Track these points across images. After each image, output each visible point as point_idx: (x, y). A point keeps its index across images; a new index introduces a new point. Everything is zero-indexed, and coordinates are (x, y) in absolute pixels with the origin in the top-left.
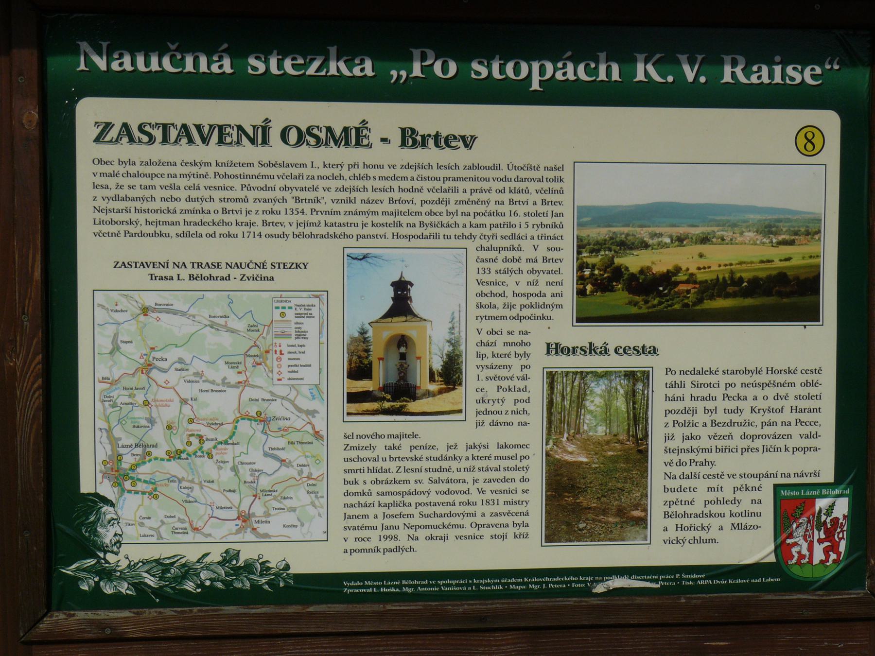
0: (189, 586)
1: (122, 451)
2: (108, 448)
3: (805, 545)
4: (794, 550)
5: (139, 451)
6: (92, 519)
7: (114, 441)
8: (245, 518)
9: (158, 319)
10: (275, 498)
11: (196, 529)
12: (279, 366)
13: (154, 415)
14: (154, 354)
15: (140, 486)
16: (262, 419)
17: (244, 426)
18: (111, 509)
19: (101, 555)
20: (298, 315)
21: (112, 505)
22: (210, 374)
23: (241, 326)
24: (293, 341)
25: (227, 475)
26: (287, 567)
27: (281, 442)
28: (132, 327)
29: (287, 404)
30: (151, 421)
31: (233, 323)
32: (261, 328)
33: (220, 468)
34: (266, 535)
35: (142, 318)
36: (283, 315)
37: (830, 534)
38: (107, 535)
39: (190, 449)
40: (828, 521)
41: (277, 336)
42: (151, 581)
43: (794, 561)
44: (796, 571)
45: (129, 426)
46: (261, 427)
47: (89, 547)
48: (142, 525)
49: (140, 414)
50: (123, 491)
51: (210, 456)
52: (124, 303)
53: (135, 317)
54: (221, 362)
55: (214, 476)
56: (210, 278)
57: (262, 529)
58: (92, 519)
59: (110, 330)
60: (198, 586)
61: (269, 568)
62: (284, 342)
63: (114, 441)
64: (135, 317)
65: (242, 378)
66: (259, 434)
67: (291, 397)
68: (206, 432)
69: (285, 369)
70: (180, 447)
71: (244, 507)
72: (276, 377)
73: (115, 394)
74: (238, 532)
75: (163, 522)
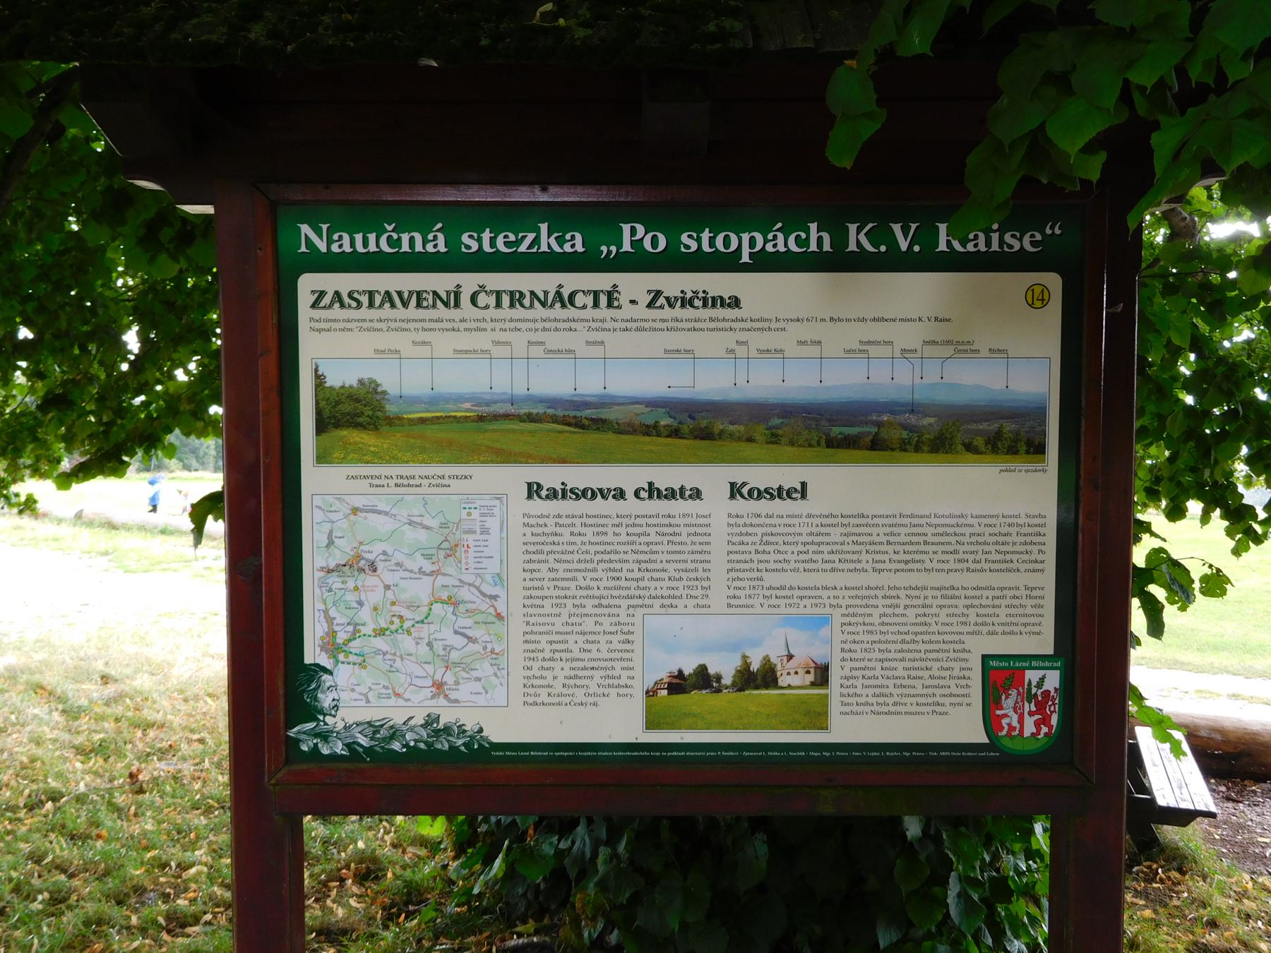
0: (396, 746)
1: (336, 628)
2: (325, 625)
3: (1015, 718)
4: (1004, 722)
5: (350, 628)
6: (313, 686)
7: (330, 620)
8: (439, 686)
9: (365, 518)
10: (464, 670)
11: (398, 695)
12: (467, 558)
13: (363, 598)
14: (362, 547)
15: (352, 658)
16: (453, 602)
17: (437, 608)
18: (330, 677)
19: (321, 718)
20: (482, 515)
21: (331, 673)
22: (409, 564)
23: (434, 523)
24: (478, 536)
25: (423, 649)
26: (481, 730)
27: (468, 622)
28: (344, 524)
29: (473, 589)
30: (360, 603)
31: (428, 521)
32: (450, 525)
33: (417, 643)
34: (456, 701)
35: (352, 517)
36: (469, 514)
37: (1041, 707)
38: (326, 700)
39: (393, 627)
40: (1039, 693)
41: (465, 532)
42: (364, 741)
43: (1004, 732)
44: (1007, 743)
45: (342, 607)
46: (451, 609)
47: (311, 712)
48: (353, 690)
49: (351, 597)
50: (337, 662)
51: (409, 632)
52: (337, 505)
53: (346, 517)
54: (418, 554)
55: (413, 651)
56: (409, 485)
57: (453, 695)
58: (313, 686)
59: (327, 527)
60: (404, 746)
61: (465, 731)
62: (470, 537)
63: (330, 620)
64: (346, 517)
65: (435, 568)
66: (449, 615)
67: (477, 584)
68: (406, 613)
69: (471, 560)
70: (384, 625)
71: (438, 677)
72: (464, 567)
73: (330, 581)
74: (433, 697)
75: (370, 689)
